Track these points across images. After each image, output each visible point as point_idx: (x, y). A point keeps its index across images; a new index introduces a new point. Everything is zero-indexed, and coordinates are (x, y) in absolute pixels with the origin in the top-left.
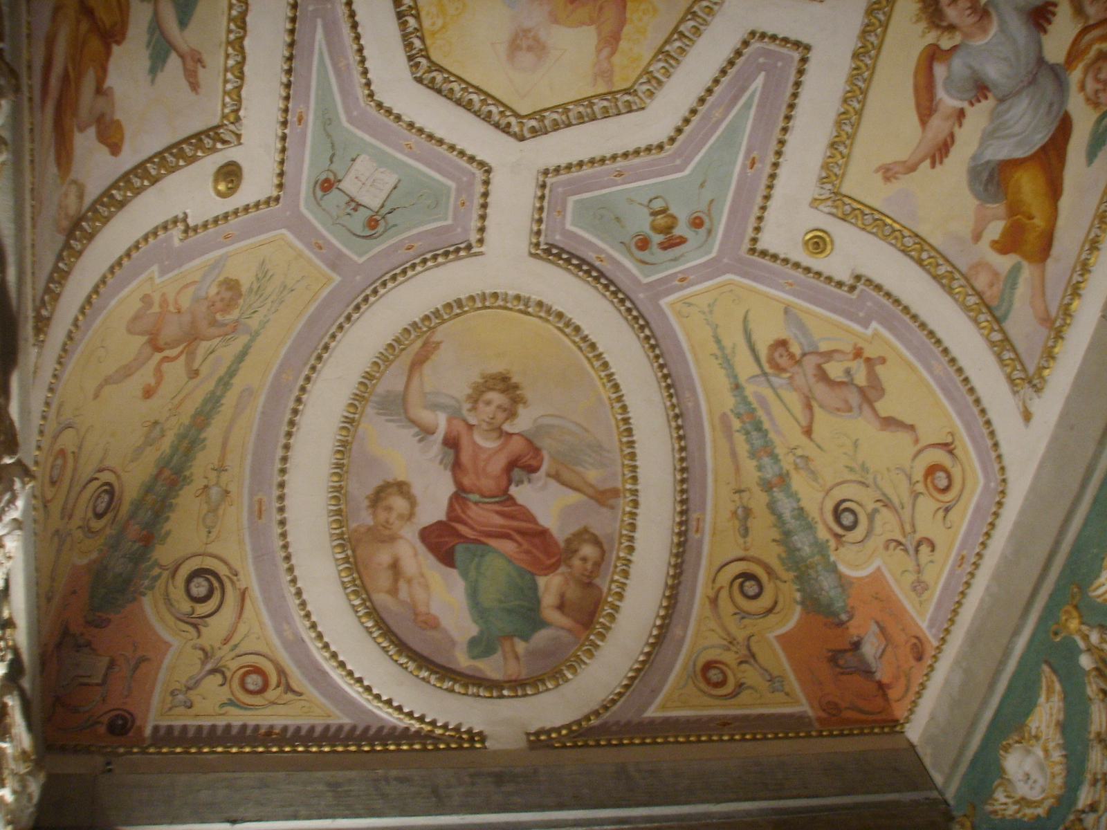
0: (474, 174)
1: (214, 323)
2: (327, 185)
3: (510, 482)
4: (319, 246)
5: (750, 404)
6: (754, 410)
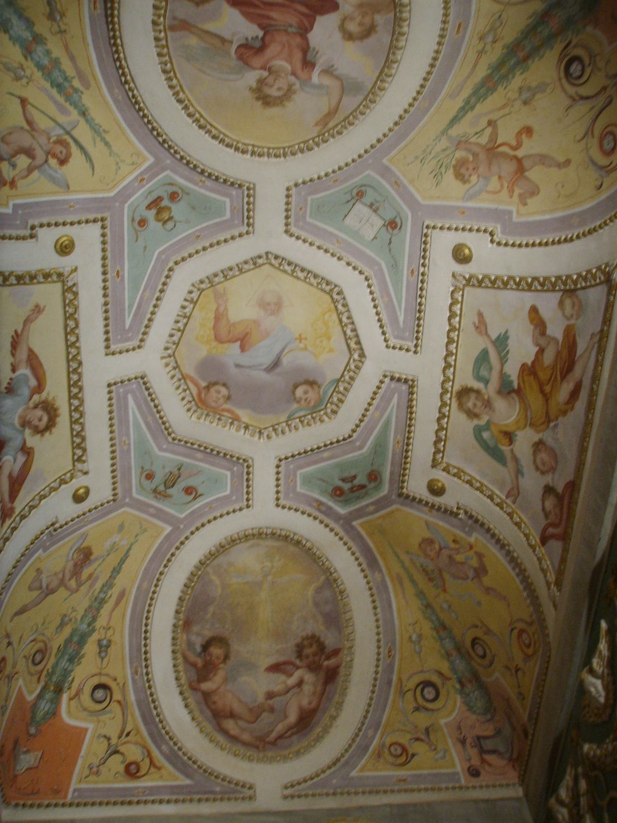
1: (475, 155)
2: (393, 225)
3: (263, 39)
4: (397, 184)
5: (71, 104)
6: (66, 101)
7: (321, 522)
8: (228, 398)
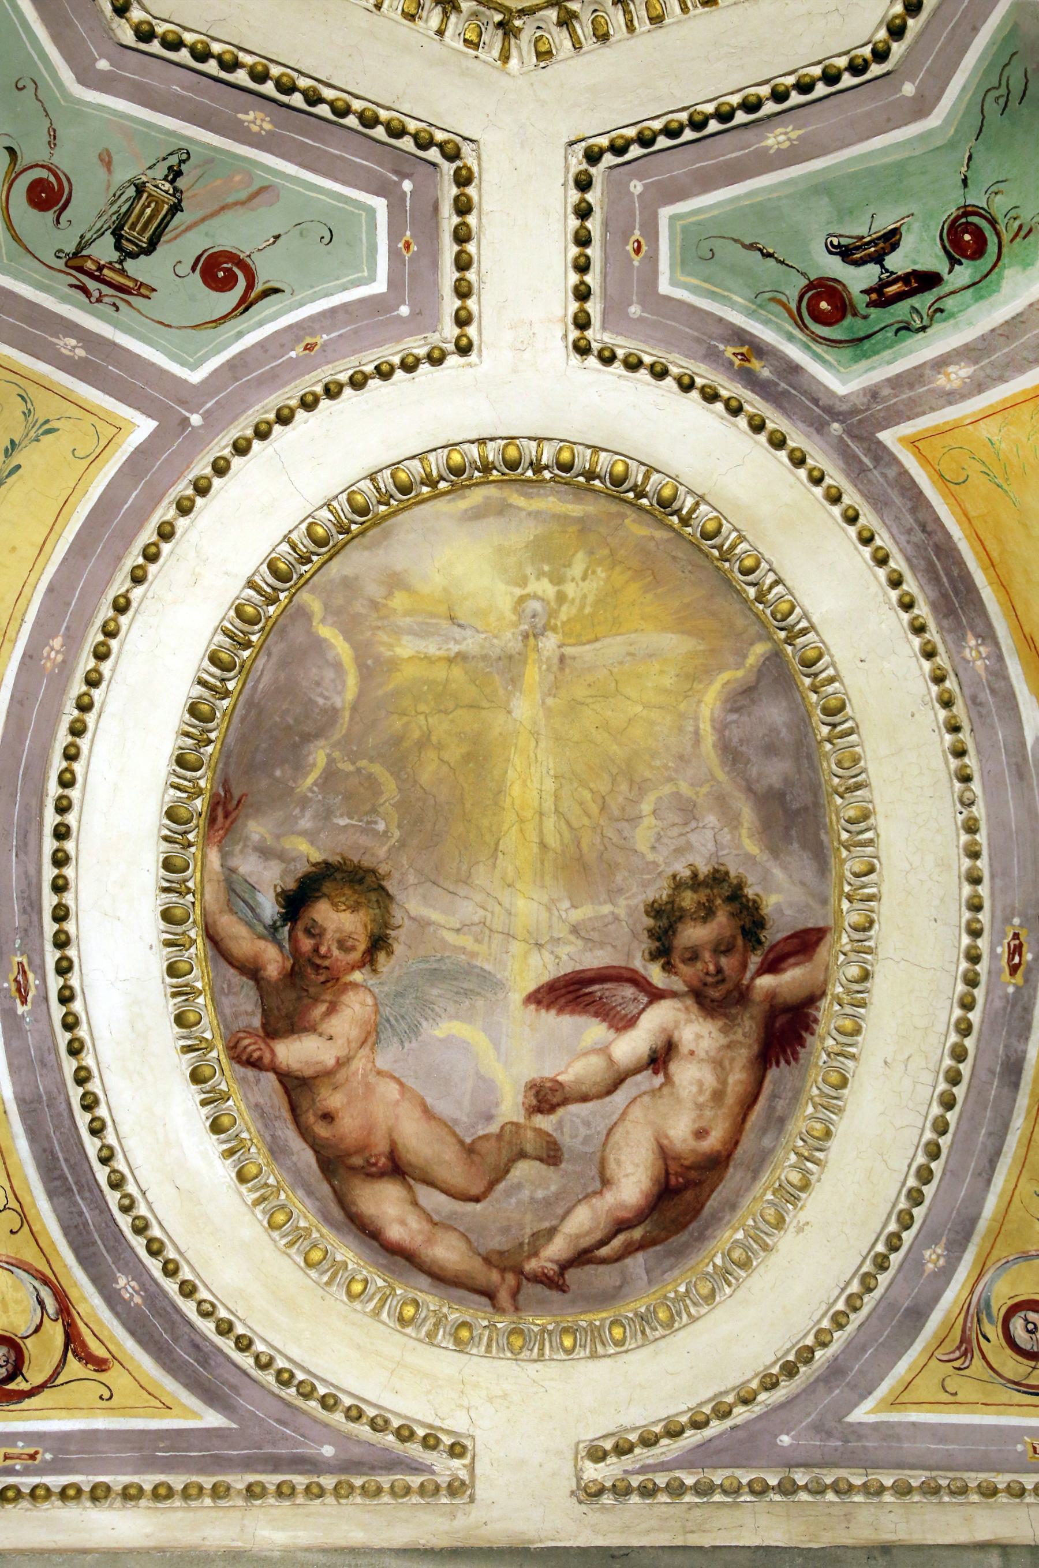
7: (757, 426)
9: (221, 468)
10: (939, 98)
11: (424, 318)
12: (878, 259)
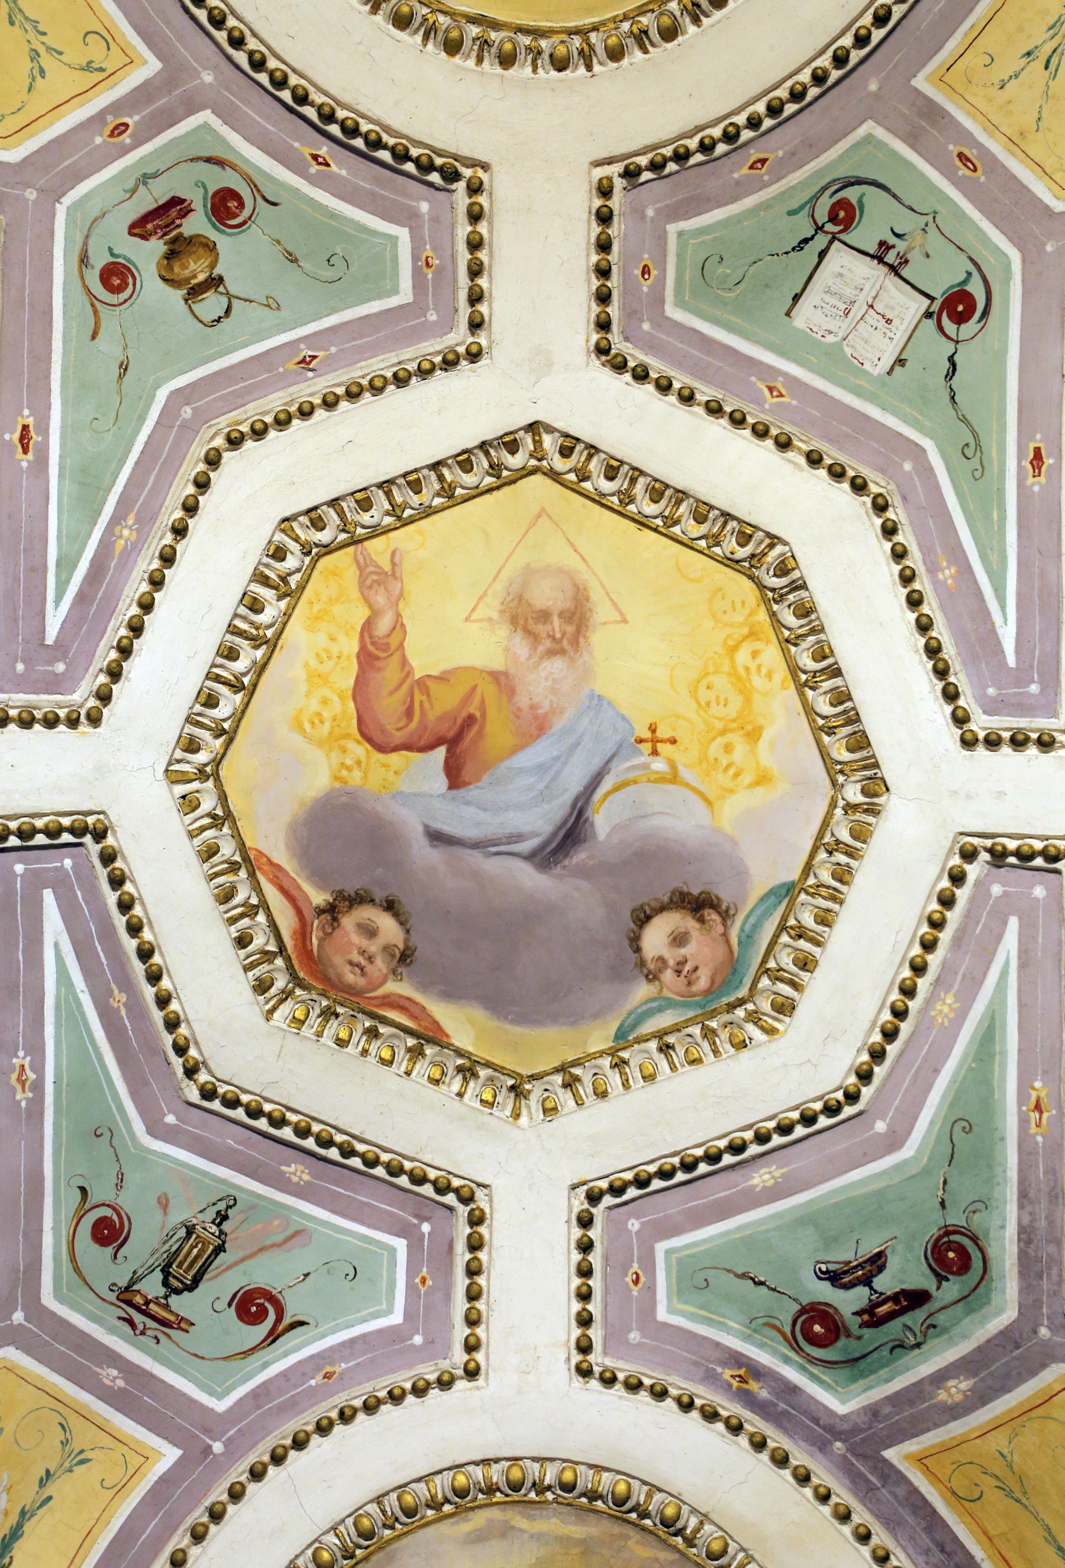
0: (627, 339)
8: (405, 957)
9: (236, 1494)
10: (909, 1133)
11: (435, 1346)
12: (867, 1281)
